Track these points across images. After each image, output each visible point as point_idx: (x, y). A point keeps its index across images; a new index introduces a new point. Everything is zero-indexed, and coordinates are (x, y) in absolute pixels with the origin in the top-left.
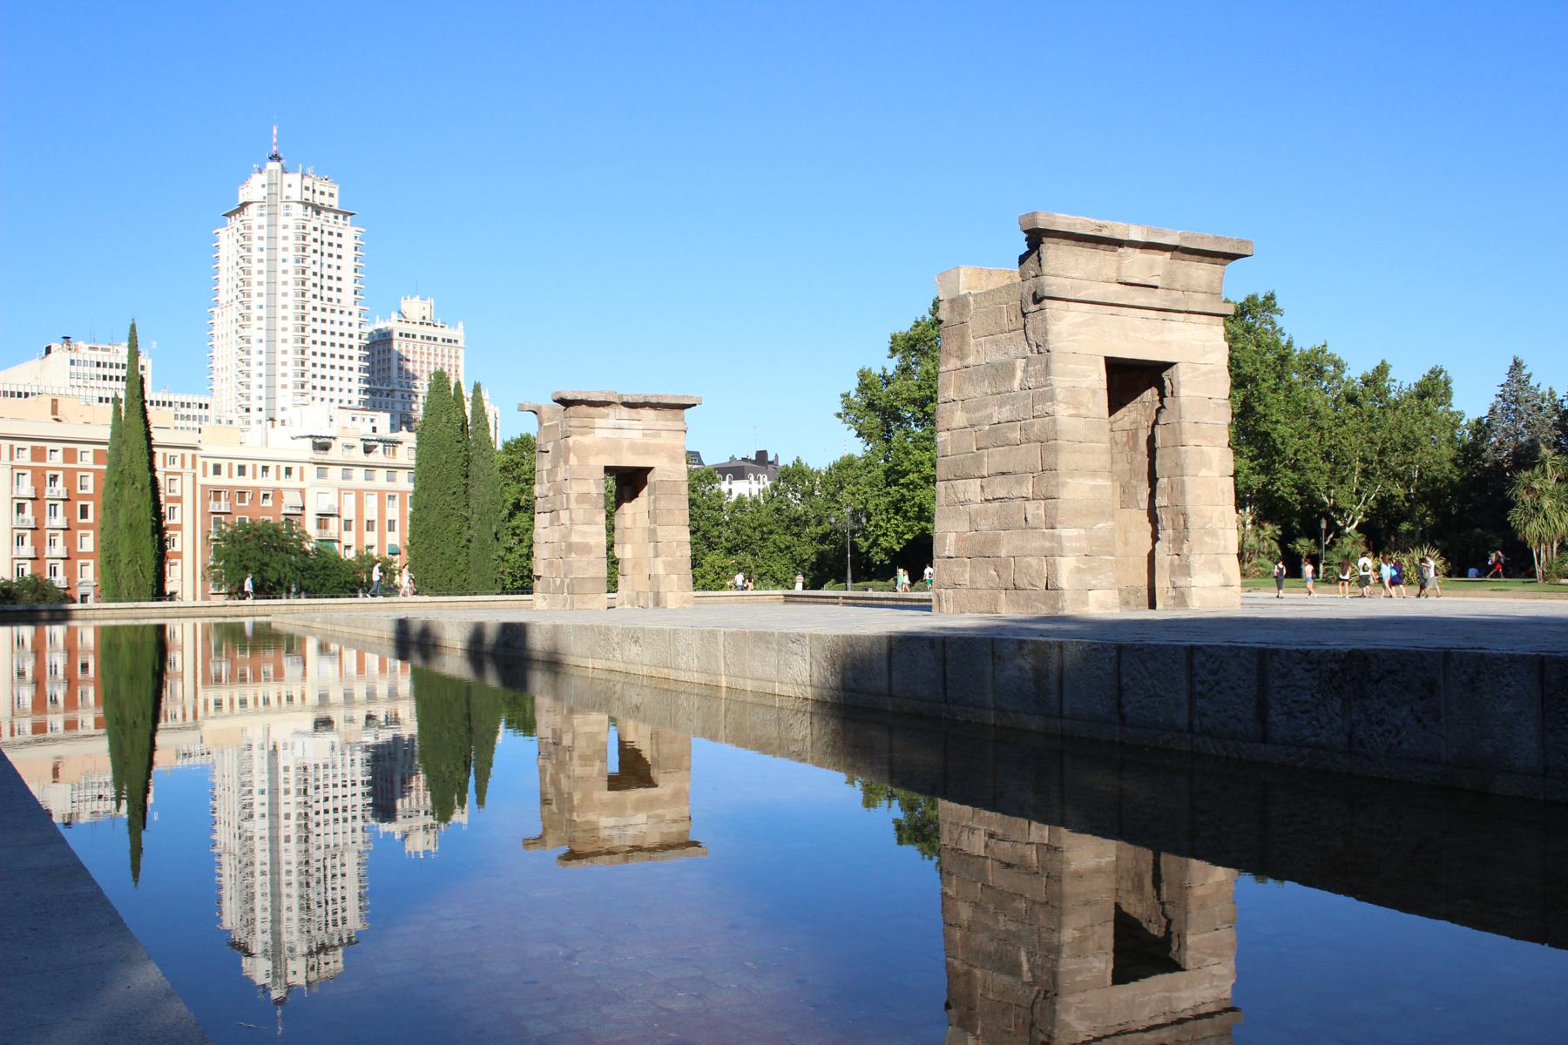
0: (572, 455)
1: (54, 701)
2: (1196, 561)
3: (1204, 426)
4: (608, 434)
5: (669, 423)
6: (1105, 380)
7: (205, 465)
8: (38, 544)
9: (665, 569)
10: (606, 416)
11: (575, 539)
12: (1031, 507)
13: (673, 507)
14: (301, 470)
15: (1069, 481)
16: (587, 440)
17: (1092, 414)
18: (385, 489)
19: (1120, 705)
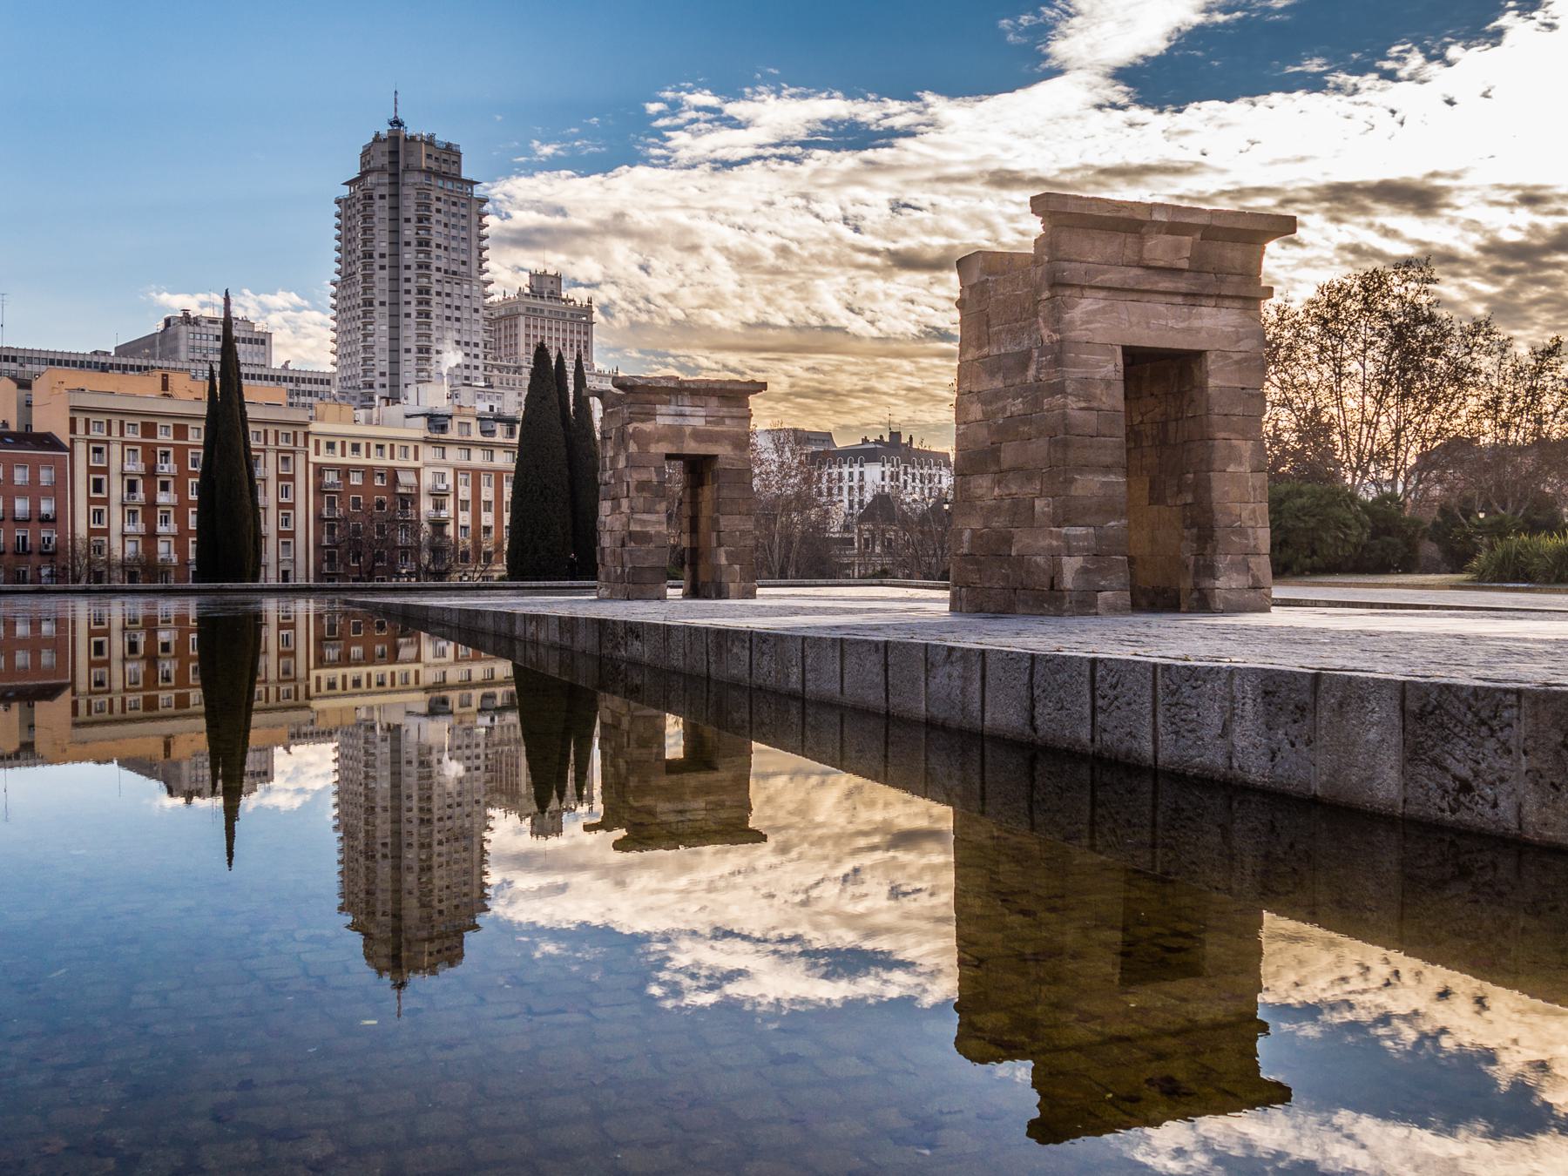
1: (168, 679)
2: (1222, 562)
3: (1235, 419)
4: (668, 421)
10: (668, 403)
13: (736, 496)
14: (416, 448)
16: (647, 427)
19: (1033, 718)
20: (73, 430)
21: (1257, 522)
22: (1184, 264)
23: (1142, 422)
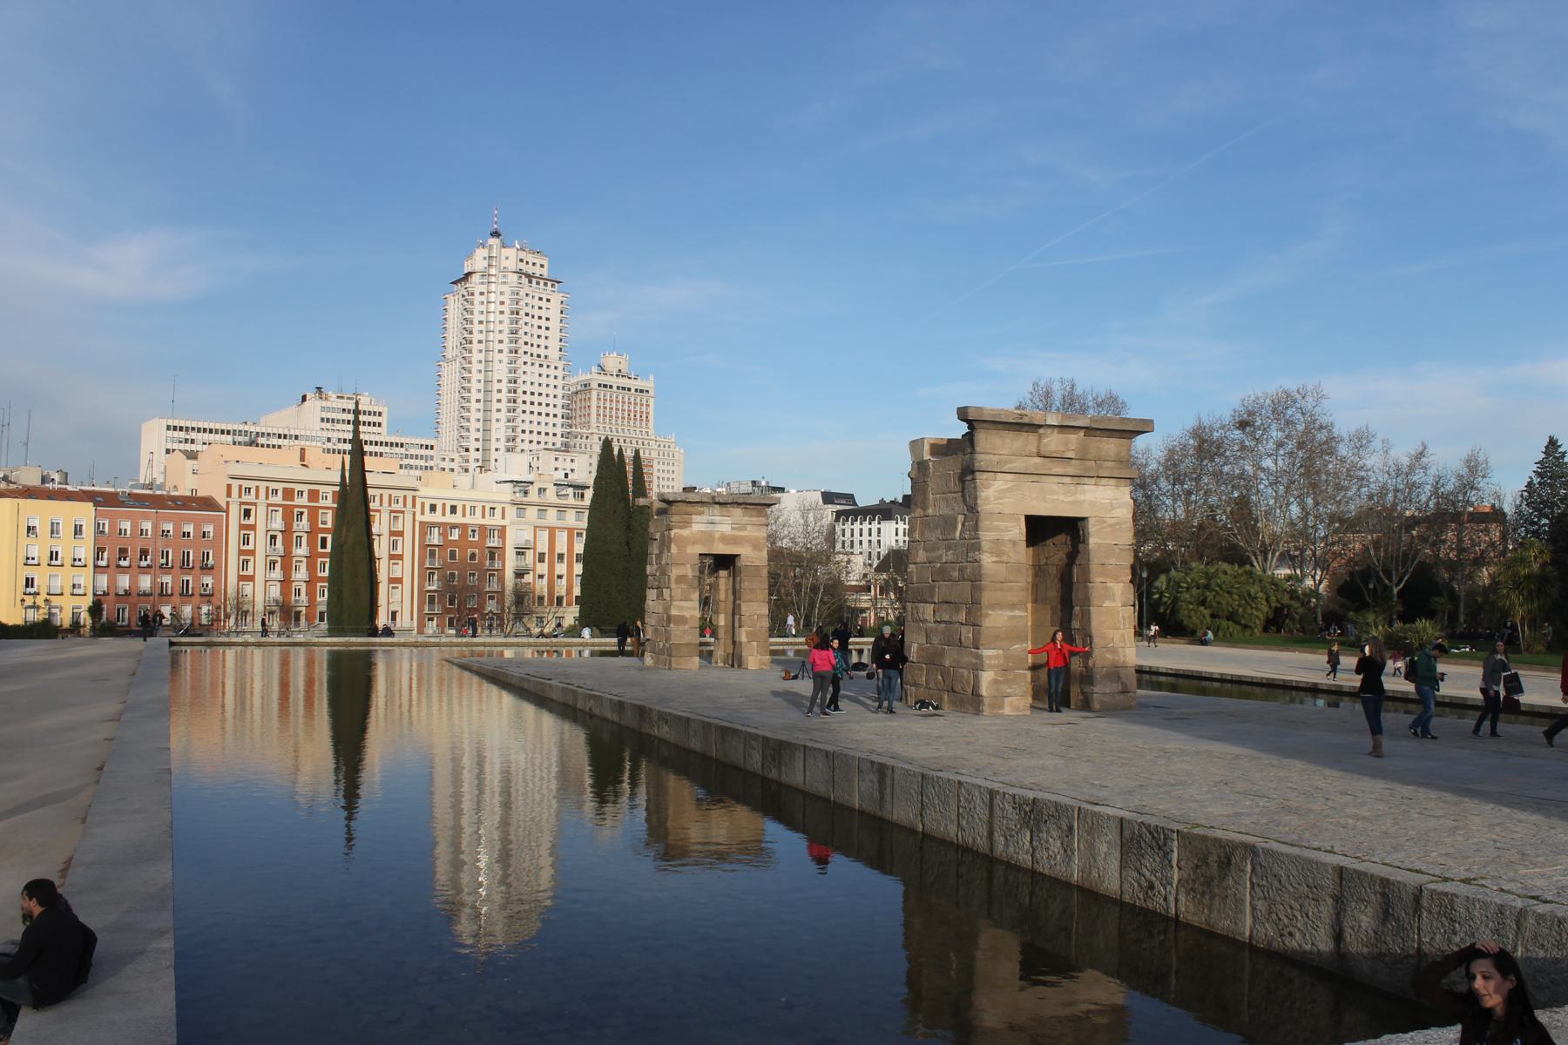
0: (672, 545)
3: (1109, 567)
4: (702, 527)
5: (754, 519)
6: (1025, 533)
7: (423, 504)
8: (287, 568)
9: (747, 637)
10: (701, 513)
11: (674, 612)
12: (964, 629)
13: (755, 587)
14: (503, 509)
15: (990, 612)
16: (685, 532)
17: (1011, 561)
20: (229, 494)
21: (1126, 644)
23: (1046, 564)
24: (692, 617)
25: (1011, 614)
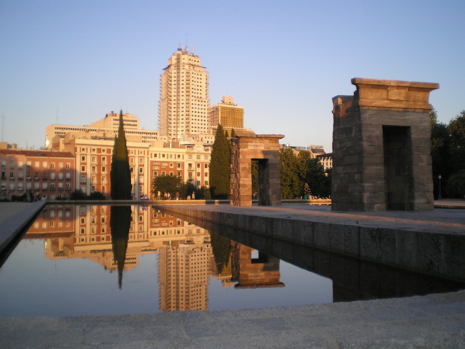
1: (103, 231)
2: (417, 194)
4: (252, 148)
5: (273, 144)
6: (382, 133)
7: (151, 154)
10: (252, 142)
14: (183, 156)
15: (367, 167)
16: (245, 150)
18: (204, 162)
22: (402, 99)
24: (249, 184)
25: (377, 168)
